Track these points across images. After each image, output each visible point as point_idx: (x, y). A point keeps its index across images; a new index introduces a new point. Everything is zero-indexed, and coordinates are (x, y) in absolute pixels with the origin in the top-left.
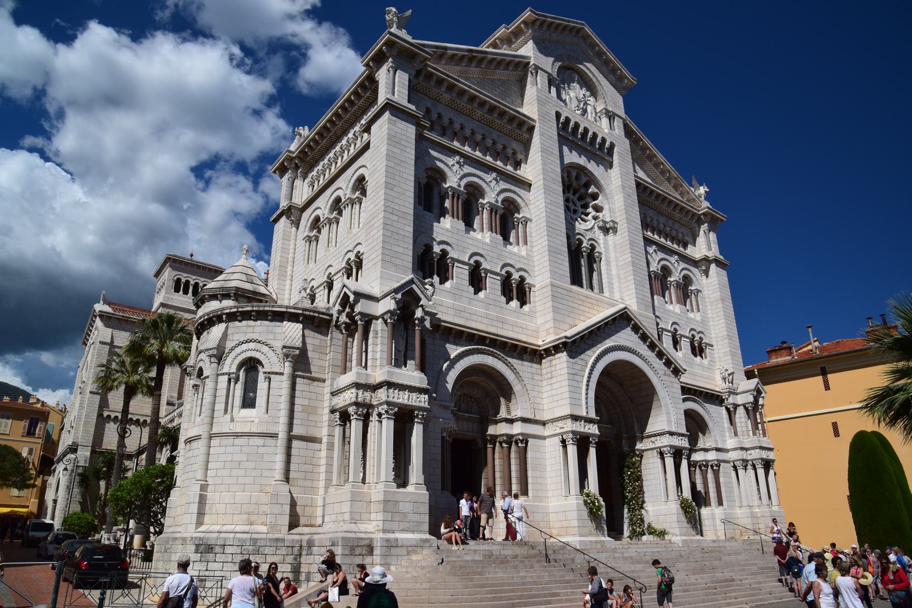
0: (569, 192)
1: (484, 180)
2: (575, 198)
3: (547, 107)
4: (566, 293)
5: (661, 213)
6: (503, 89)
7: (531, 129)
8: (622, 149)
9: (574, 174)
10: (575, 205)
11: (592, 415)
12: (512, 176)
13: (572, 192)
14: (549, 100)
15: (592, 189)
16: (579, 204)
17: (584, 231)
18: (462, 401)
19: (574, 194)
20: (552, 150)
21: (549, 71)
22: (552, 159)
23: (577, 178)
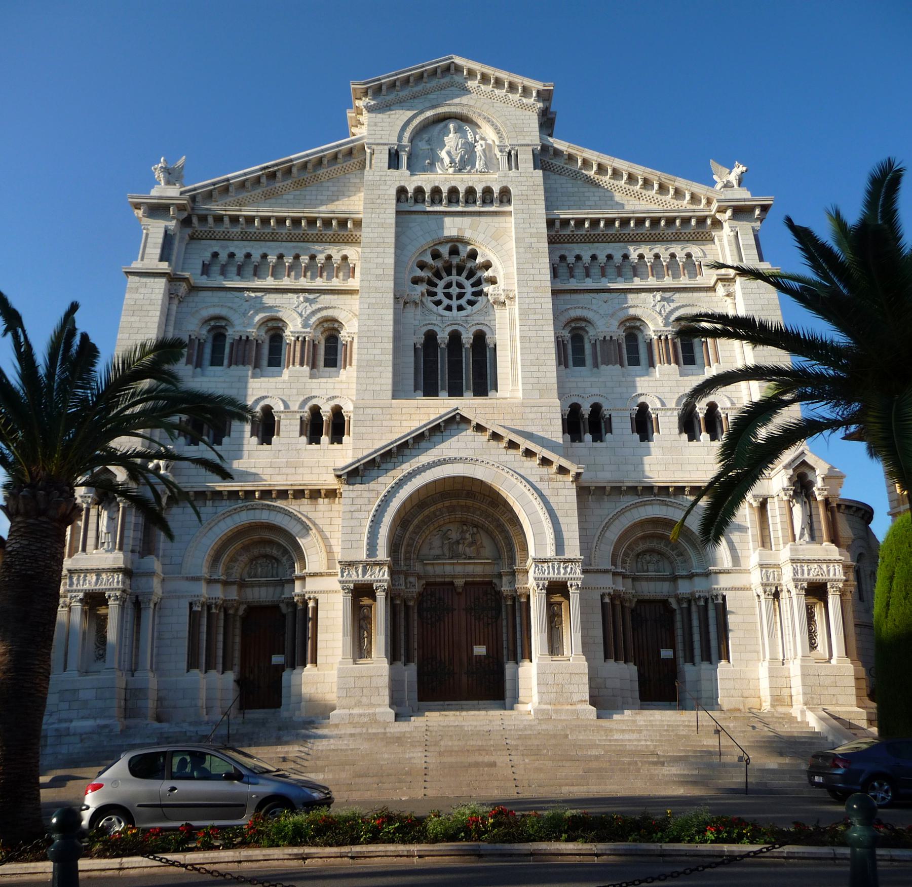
0: (449, 274)
2: (462, 279)
4: (379, 411)
6: (335, 189)
7: (358, 224)
8: (524, 188)
9: (445, 250)
10: (460, 286)
11: (382, 554)
12: (331, 290)
13: (454, 271)
14: (387, 178)
16: (467, 284)
18: (258, 565)
19: (459, 274)
20: (381, 240)
22: (381, 250)
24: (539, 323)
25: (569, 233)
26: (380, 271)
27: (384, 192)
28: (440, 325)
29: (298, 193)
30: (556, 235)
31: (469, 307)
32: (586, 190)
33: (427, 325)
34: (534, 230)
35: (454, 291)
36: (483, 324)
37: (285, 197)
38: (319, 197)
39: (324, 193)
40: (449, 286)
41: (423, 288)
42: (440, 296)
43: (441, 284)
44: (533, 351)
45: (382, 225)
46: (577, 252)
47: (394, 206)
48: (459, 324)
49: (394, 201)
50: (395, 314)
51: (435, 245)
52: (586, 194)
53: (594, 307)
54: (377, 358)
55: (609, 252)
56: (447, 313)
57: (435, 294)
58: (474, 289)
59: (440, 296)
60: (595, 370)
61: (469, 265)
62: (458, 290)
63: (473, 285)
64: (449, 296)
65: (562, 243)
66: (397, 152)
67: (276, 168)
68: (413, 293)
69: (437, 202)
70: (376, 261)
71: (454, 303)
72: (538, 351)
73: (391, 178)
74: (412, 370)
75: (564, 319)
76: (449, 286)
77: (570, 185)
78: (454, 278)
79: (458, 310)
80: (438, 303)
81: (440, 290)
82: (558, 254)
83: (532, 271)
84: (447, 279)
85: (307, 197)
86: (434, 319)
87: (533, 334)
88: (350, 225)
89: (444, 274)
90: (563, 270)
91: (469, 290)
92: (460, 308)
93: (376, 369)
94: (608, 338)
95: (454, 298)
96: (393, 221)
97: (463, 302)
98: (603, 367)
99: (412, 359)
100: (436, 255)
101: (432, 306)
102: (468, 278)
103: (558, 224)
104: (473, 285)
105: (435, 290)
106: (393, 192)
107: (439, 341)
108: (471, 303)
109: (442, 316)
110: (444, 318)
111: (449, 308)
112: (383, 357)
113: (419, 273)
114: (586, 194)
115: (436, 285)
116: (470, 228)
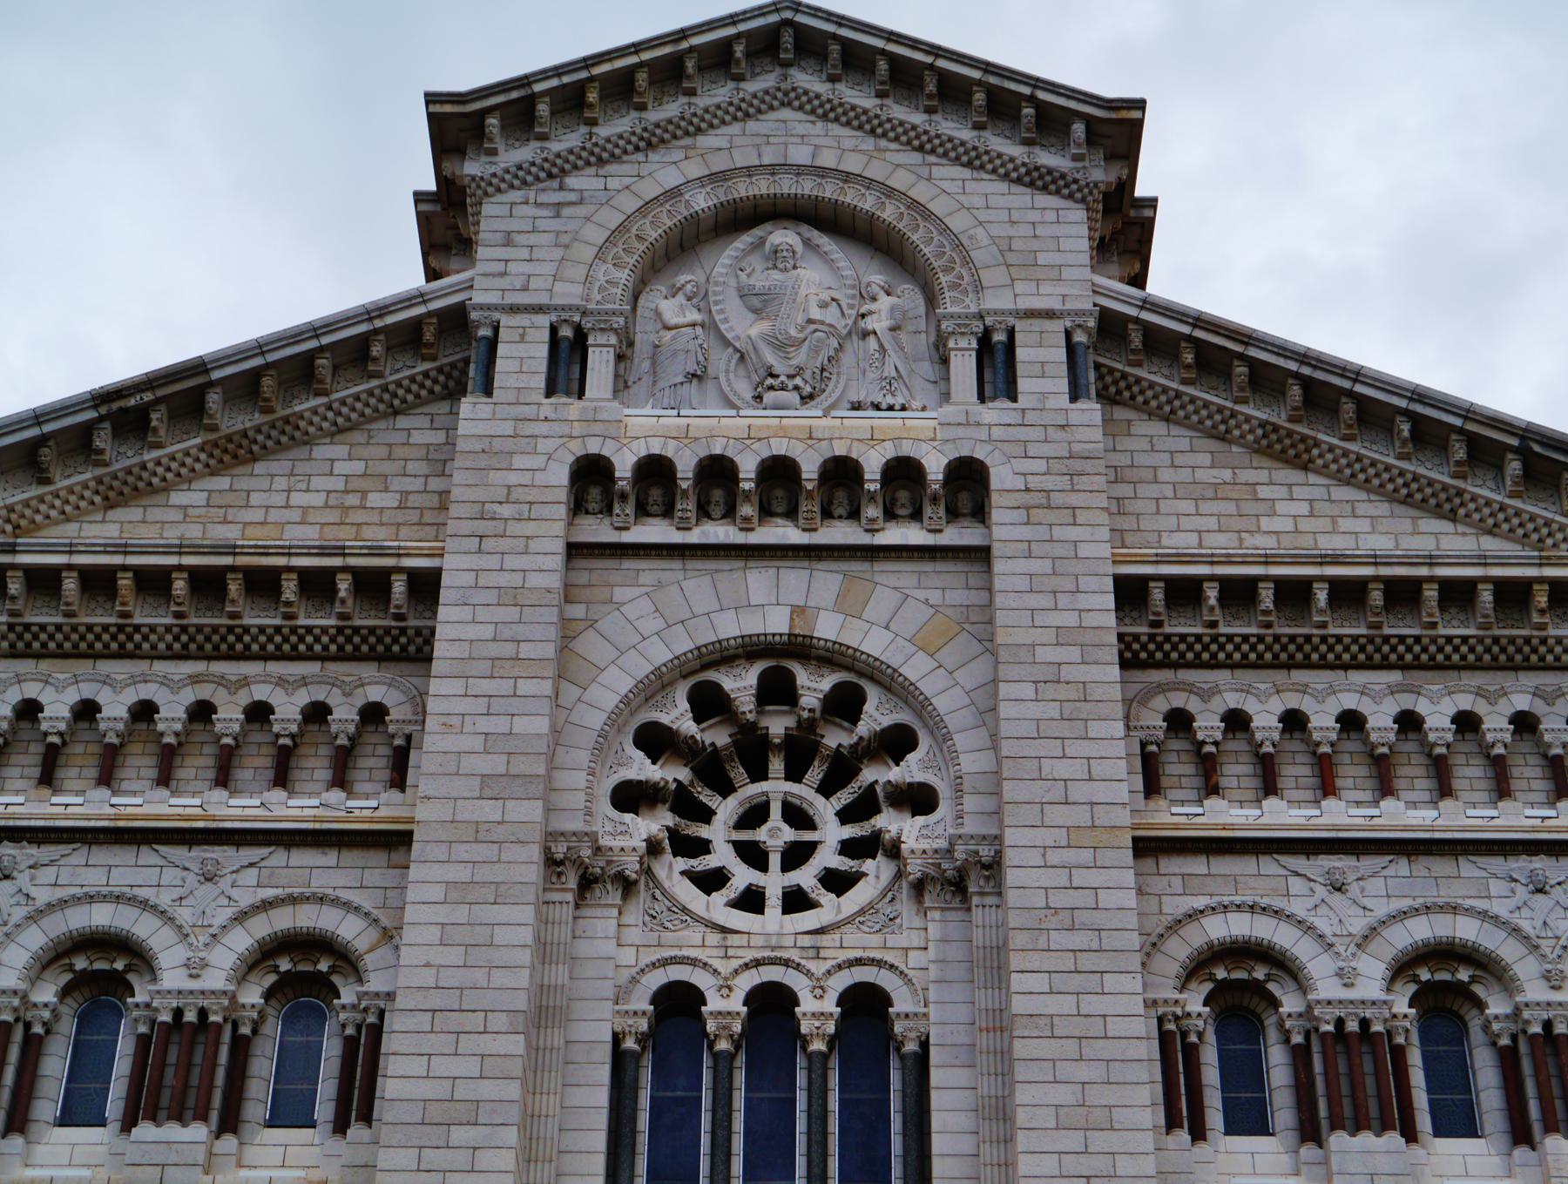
1: (145, 905)
2: (805, 792)
3: (519, 461)
5: (1433, 666)
6: (359, 467)
7: (426, 586)
8: (1040, 466)
9: (741, 684)
10: (797, 816)
13: (777, 765)
14: (541, 428)
15: (877, 714)
16: (825, 810)
17: (806, 941)
20: (508, 650)
21: (569, 293)
22: (505, 686)
23: (776, 690)
24: (1086, 962)
25: (1198, 630)
26: (496, 764)
27: (526, 478)
28: (716, 964)
29: (222, 482)
30: (1152, 637)
31: (827, 898)
32: (1263, 475)
33: (665, 962)
34: (1070, 619)
35: (776, 834)
36: (880, 963)
37: (177, 498)
38: (298, 499)
39: (317, 482)
40: (755, 815)
41: (653, 824)
42: (722, 856)
43: (727, 810)
44: (1065, 1070)
45: (511, 597)
46: (1232, 700)
47: (559, 528)
48: (786, 963)
49: (562, 511)
50: (543, 921)
51: (705, 667)
52: (1263, 492)
53: (1298, 908)
54: (463, 1091)
55: (1350, 701)
56: (740, 919)
57: (703, 847)
58: (849, 832)
59: (722, 856)
60: (1309, 1151)
61: (835, 738)
62: (789, 834)
63: (845, 816)
64: (754, 855)
65: (1175, 666)
66: (580, 342)
67: (148, 397)
68: (616, 843)
69: (717, 511)
70: (485, 724)
71: (774, 883)
72: (1084, 1072)
73: (557, 428)
74: (599, 1141)
75: (1180, 950)
76: (755, 815)
77: (1205, 459)
78: (776, 787)
79: (787, 909)
80: (711, 881)
81: (719, 832)
82: (1162, 704)
83: (1062, 769)
84: (750, 791)
85: (255, 499)
86: (691, 940)
87: (1066, 1004)
88: (399, 586)
89: (738, 773)
90: (1178, 768)
91: (831, 832)
92: (796, 901)
93: (459, 1135)
94: (1352, 1026)
95: (775, 860)
96: (554, 581)
97: (805, 877)
98: (1338, 1140)
99: (602, 1097)
100: (709, 703)
101: (688, 893)
102: (826, 789)
103: (1157, 594)
104: (845, 816)
105: (704, 832)
106: (560, 475)
107: (711, 1026)
108: (837, 882)
109: (724, 930)
110: (733, 940)
111: (752, 901)
112: (487, 1090)
113: (641, 768)
114: (1263, 492)
115: (706, 815)
116: (839, 606)
